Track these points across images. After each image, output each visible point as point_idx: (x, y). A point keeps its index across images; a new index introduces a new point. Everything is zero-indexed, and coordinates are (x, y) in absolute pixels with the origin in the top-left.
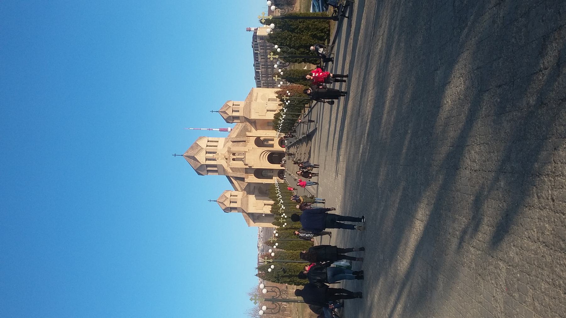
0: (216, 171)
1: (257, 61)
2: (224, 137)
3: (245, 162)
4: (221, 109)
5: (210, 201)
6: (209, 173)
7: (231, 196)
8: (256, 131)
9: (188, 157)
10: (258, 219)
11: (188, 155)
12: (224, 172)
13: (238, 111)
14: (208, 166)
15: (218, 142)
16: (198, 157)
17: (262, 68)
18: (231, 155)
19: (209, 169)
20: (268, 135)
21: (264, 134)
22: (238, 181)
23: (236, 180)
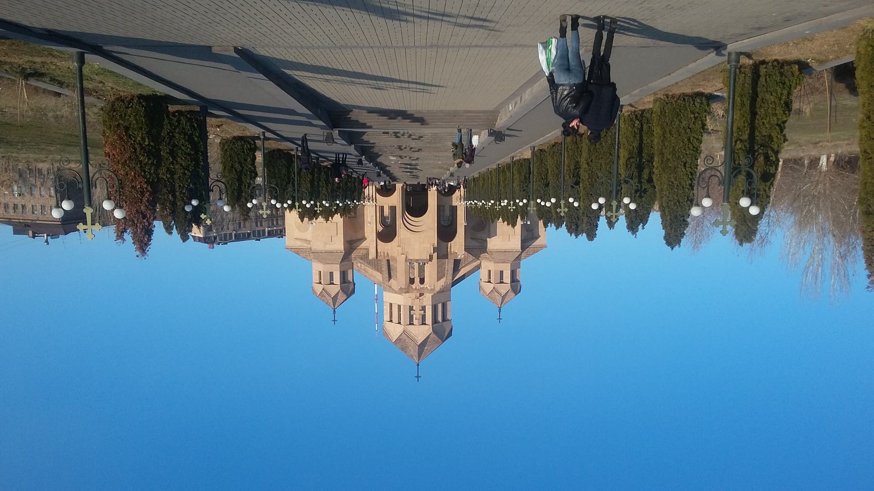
0: (444, 306)
1: (249, 234)
2: (383, 293)
3: (427, 260)
4: (329, 305)
5: (500, 319)
6: (448, 317)
7: (489, 282)
8: (366, 239)
9: (420, 355)
10: (533, 230)
11: (417, 355)
12: (445, 292)
13: (331, 274)
14: (435, 321)
15: (391, 305)
16: (420, 338)
17: (262, 226)
18: (414, 286)
19: (440, 319)
20: (372, 216)
21: (371, 226)
22: (461, 266)
23: (460, 270)
